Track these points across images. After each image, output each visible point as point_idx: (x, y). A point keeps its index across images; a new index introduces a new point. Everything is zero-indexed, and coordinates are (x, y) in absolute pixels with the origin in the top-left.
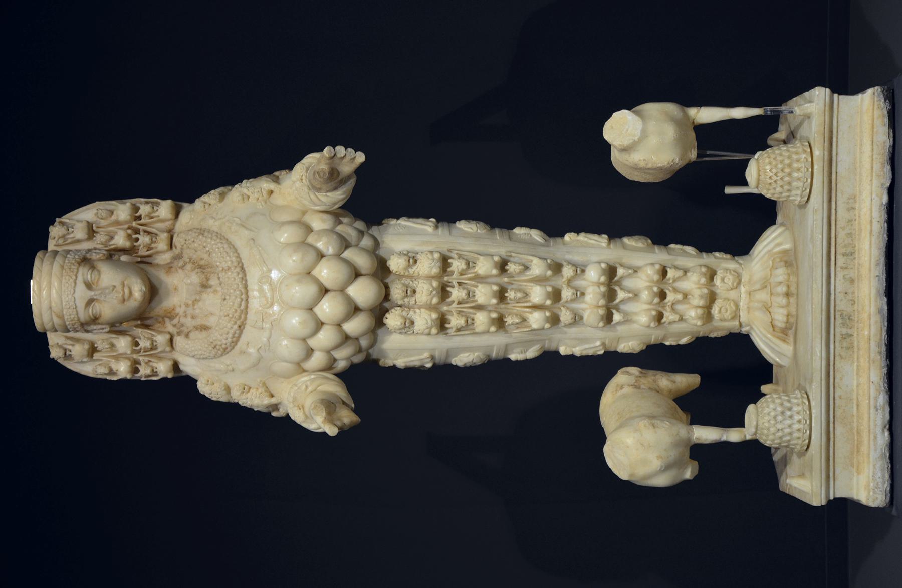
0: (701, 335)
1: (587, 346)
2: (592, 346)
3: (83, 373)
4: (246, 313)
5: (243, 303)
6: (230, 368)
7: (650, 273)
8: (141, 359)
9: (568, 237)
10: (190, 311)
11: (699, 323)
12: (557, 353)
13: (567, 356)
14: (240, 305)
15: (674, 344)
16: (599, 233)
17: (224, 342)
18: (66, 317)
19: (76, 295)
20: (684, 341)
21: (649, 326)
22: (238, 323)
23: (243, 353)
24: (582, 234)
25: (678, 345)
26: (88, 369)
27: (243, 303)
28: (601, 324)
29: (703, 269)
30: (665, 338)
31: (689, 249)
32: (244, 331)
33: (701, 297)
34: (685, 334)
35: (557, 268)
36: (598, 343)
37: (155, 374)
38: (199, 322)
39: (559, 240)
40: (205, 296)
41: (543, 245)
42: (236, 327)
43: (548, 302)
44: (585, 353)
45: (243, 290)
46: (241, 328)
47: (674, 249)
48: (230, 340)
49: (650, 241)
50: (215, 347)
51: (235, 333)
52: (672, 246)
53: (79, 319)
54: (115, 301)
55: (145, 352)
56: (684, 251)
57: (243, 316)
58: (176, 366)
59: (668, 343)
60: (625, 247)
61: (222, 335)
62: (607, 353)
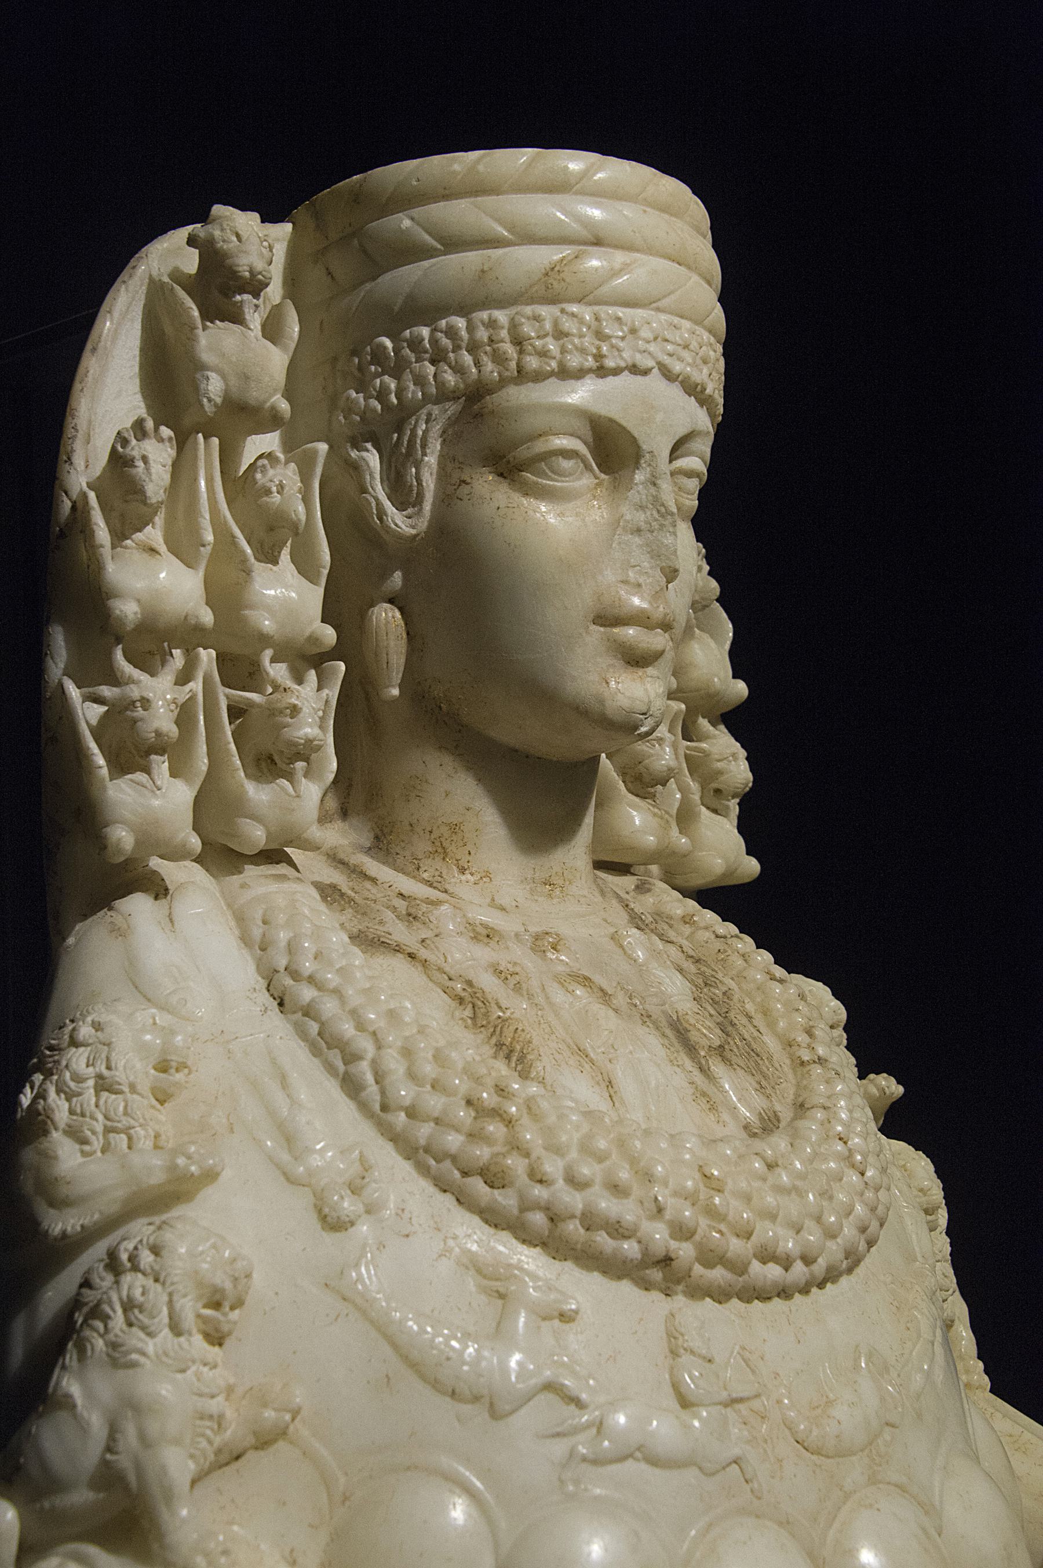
3: (90, 364)
4: (721, 1295)
5: (774, 1272)
6: (348, 1206)
8: (196, 686)
10: (529, 963)
14: (766, 1256)
17: (553, 1167)
18: (545, 311)
19: (655, 381)
22: (685, 1251)
23: (498, 1287)
26: (109, 395)
27: (774, 1272)
32: (626, 1287)
37: (131, 754)
38: (518, 1008)
40: (653, 1040)
42: (659, 1235)
45: (821, 1265)
46: (658, 1272)
48: (574, 1201)
50: (496, 1113)
51: (618, 1230)
53: (522, 376)
54: (609, 576)
55: (236, 712)
57: (718, 1275)
58: (133, 878)
61: (586, 1149)
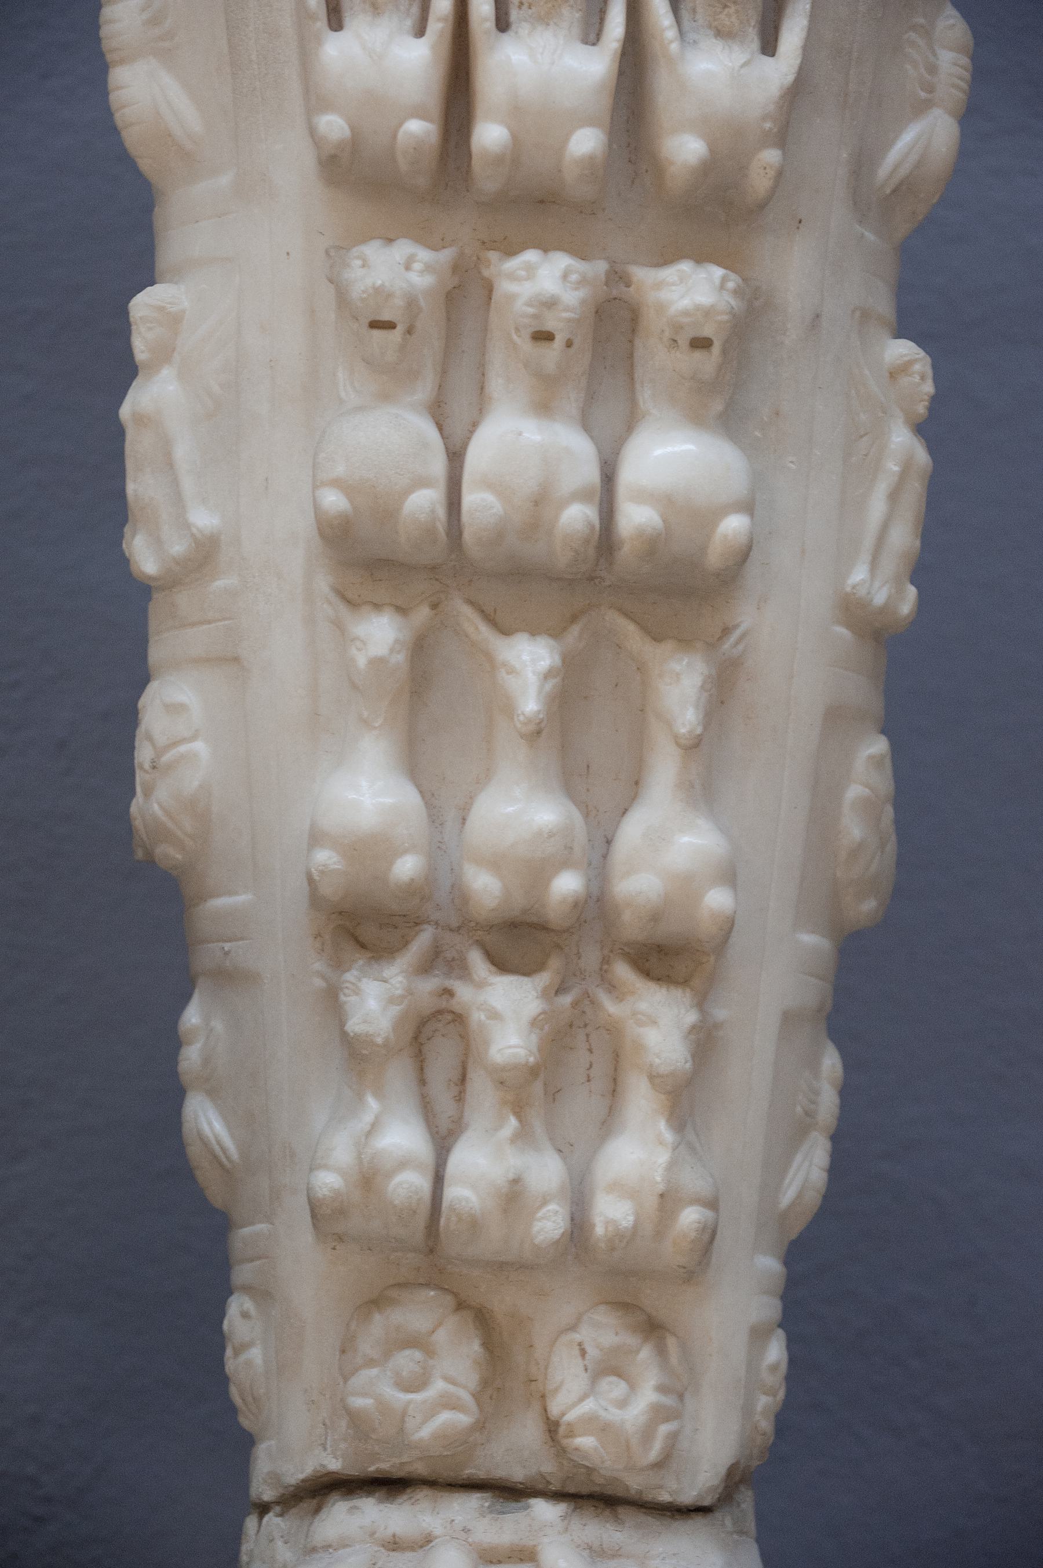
0: (246, 1235)
1: (183, 451)
2: (188, 485)
7: (669, 848)
9: (903, 349)
11: (328, 1181)
12: (144, 273)
13: (121, 329)
15: (191, 1057)
16: (922, 571)
20: (206, 1121)
21: (316, 838)
24: (922, 456)
25: (172, 1094)
28: (333, 501)
29: (690, 1217)
30: (232, 978)
31: (809, 1169)
33: (513, 1197)
34: (249, 1121)
35: (717, 215)
36: (203, 519)
39: (884, 305)
41: (862, 163)
43: (490, 135)
44: (138, 445)
47: (813, 1064)
49: (866, 908)
52: (831, 1062)
56: (802, 1130)
59: (192, 1016)
60: (836, 718)
62: (138, 594)
